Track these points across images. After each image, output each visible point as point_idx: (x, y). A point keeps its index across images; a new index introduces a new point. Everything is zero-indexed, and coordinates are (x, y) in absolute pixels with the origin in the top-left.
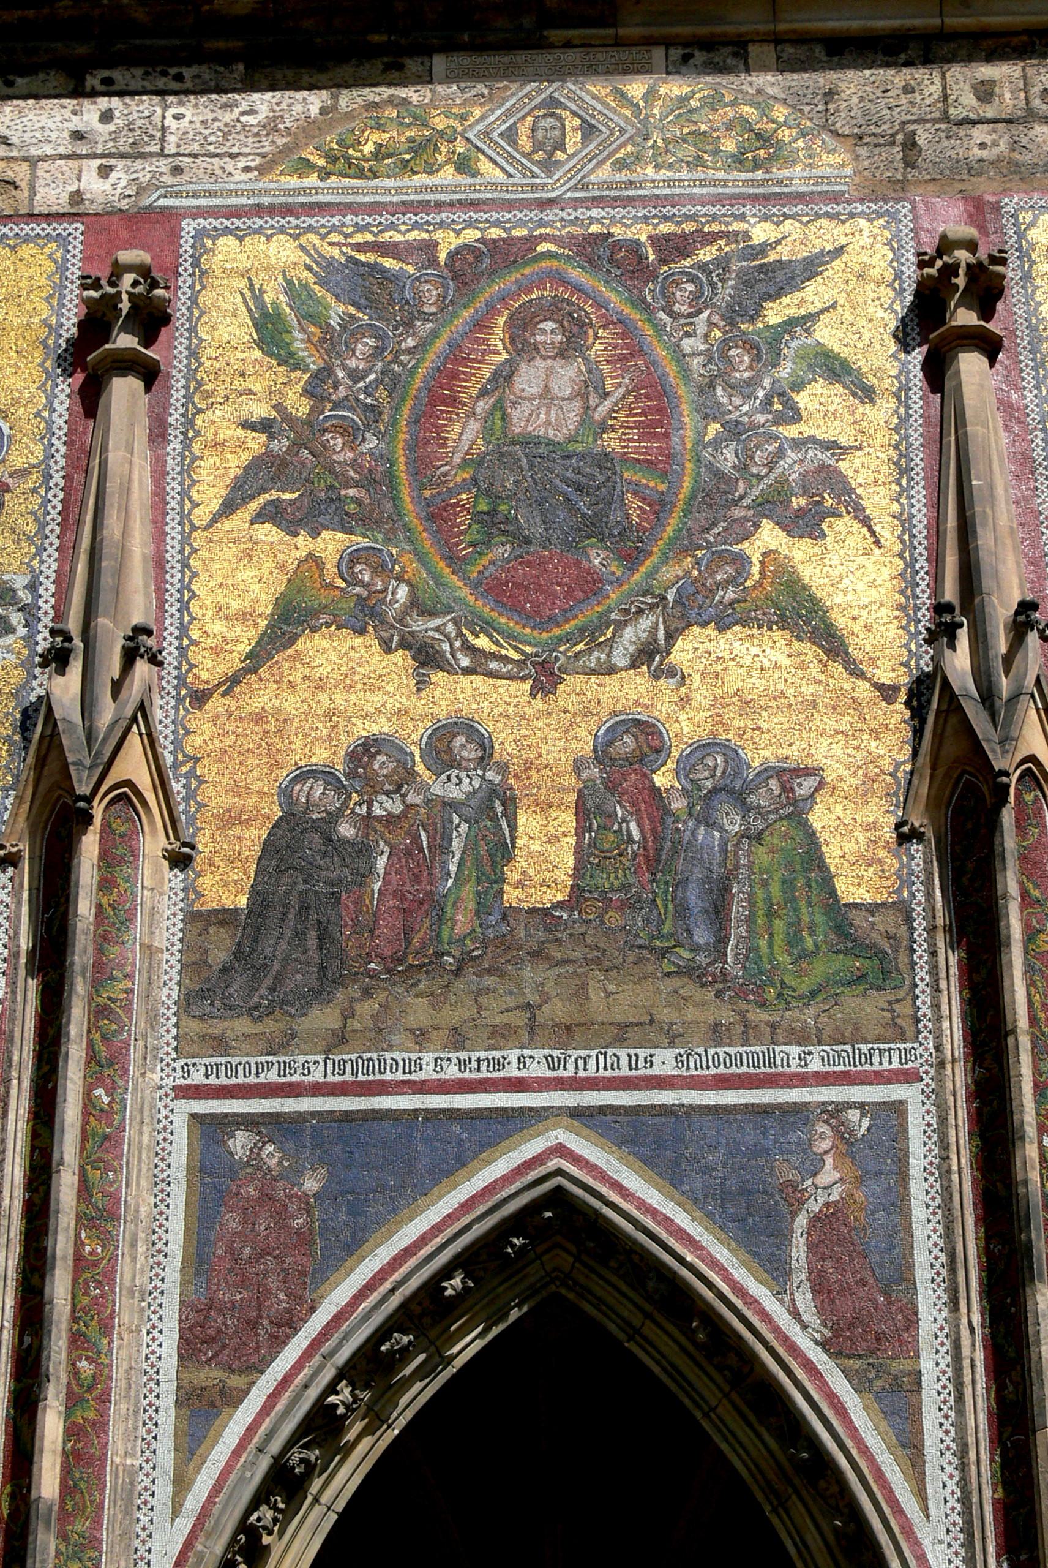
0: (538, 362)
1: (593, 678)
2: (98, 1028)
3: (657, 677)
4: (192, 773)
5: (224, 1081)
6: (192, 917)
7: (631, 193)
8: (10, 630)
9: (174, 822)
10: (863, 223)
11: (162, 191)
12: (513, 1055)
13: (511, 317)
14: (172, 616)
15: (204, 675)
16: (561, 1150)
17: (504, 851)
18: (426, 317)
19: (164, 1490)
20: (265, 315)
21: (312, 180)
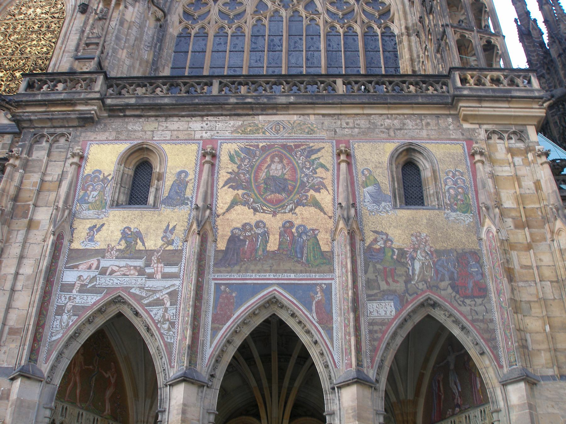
6: (216, 251)
8: (187, 204)
12: (268, 274)
16: (275, 290)
17: (267, 242)
18: (257, 156)
19: (209, 344)
21: (239, 135)
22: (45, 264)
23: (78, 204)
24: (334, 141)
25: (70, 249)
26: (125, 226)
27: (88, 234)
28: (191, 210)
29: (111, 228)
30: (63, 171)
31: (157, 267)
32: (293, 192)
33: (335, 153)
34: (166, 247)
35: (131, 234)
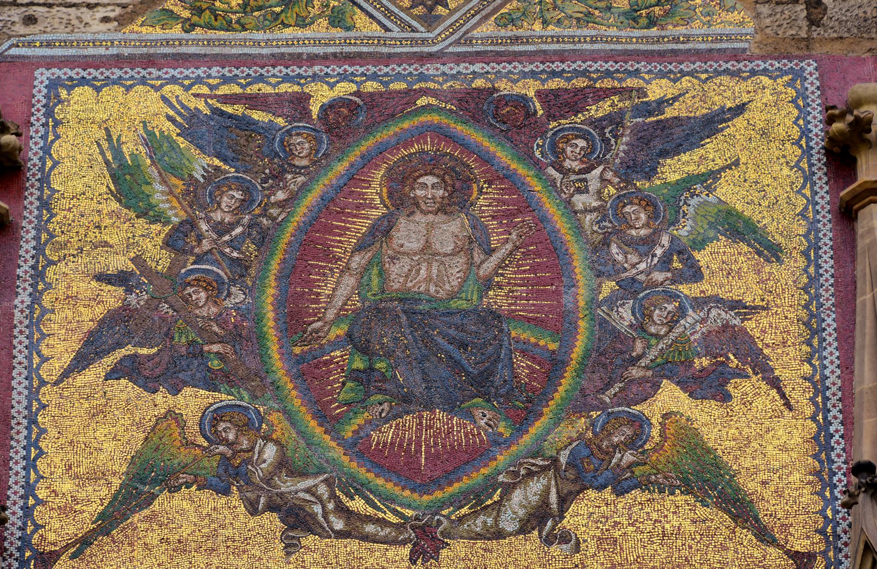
0: (418, 217)
1: (479, 543)
3: (548, 541)
7: (516, 48)
10: (765, 80)
11: (14, 41)
13: (389, 170)
14: (17, 474)
15: (51, 537)
18: (298, 171)
20: (122, 165)
21: (176, 31)
24: (810, 67)
32: (545, 396)
33: (818, 143)
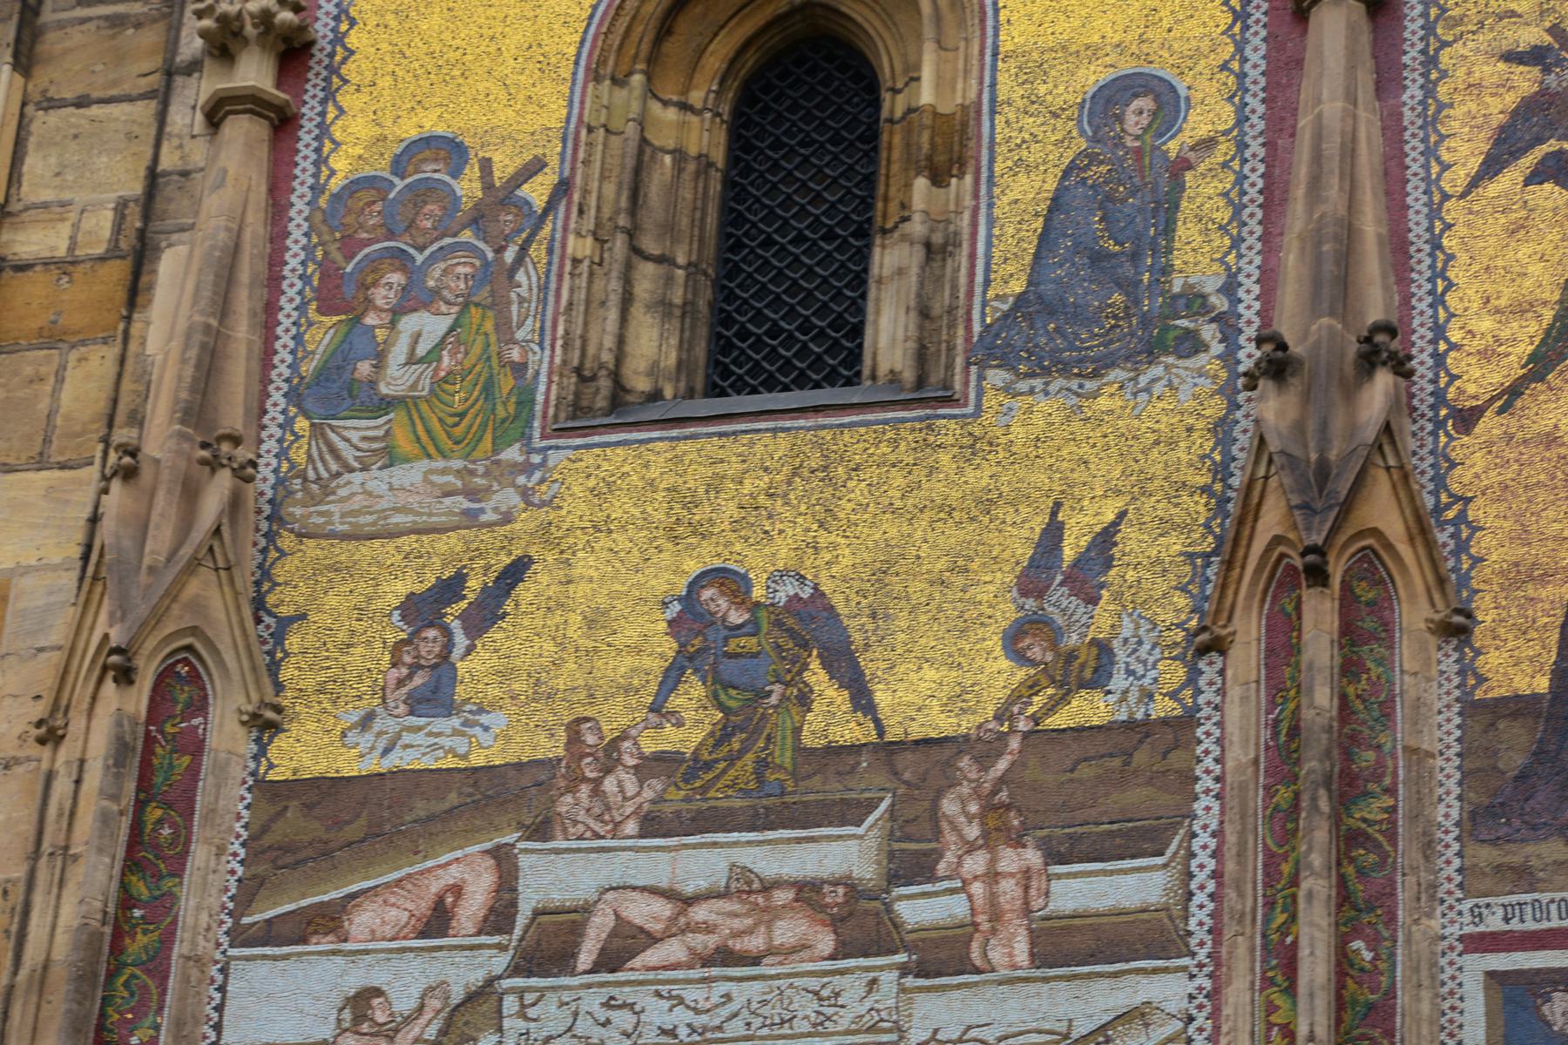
2: (1352, 860)
4: (1462, 516)
5: (1531, 925)
6: (1471, 708)
8: (1199, 347)
9: (1441, 581)
14: (1422, 313)
22: (69, 914)
23: (302, 424)
25: (264, 789)
26: (693, 567)
27: (398, 647)
28: (1227, 392)
29: (580, 590)
30: (153, 177)
31: (992, 876)
34: (1052, 708)
35: (752, 628)
